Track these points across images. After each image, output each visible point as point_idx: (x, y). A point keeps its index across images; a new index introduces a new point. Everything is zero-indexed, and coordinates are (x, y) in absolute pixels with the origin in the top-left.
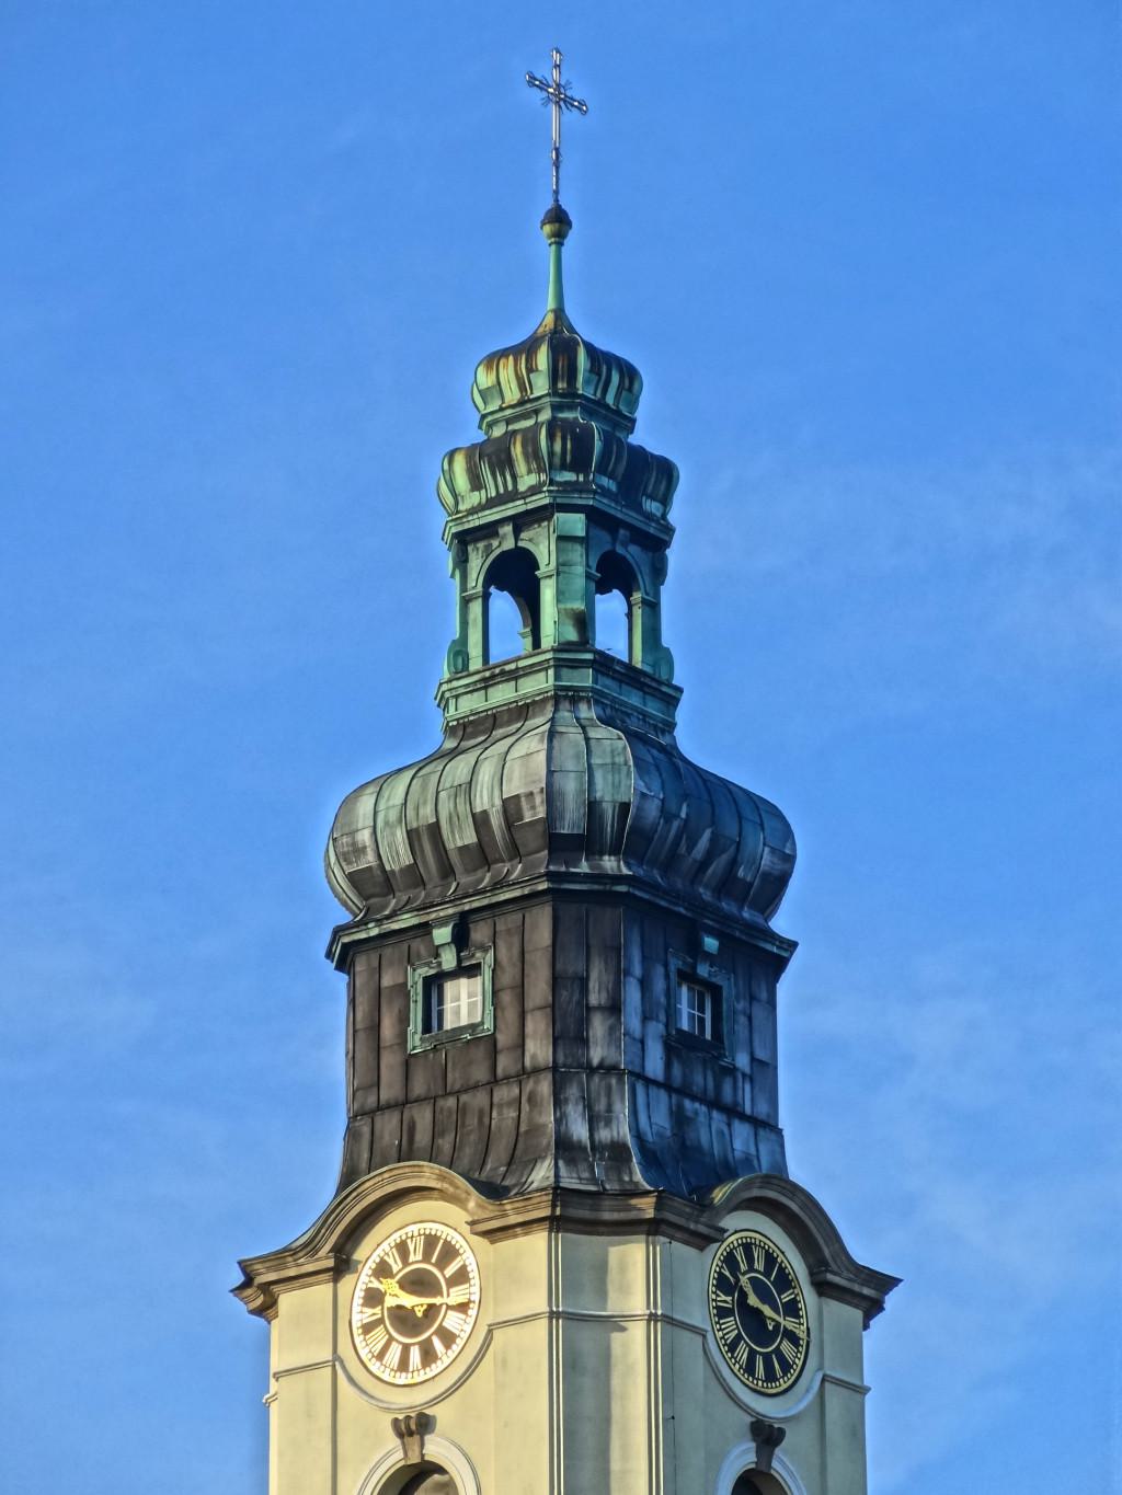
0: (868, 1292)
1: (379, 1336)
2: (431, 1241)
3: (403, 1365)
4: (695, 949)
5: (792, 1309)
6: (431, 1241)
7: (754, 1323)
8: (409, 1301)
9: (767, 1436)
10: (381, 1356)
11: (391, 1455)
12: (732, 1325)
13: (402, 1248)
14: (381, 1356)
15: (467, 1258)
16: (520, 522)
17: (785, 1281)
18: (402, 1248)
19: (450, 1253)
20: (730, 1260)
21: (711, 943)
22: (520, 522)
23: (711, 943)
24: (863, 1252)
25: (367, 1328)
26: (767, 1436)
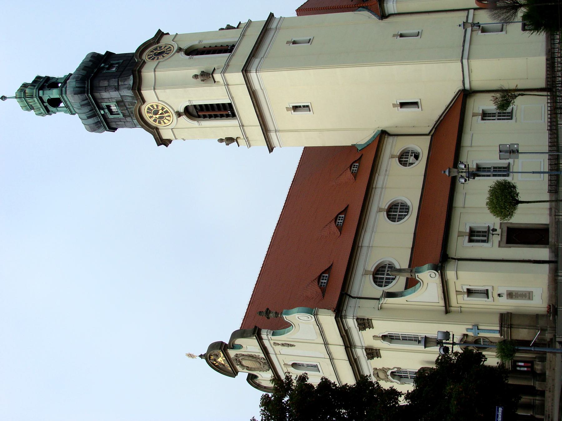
0: (160, 35)
1: (165, 121)
2: (148, 112)
3: (169, 116)
4: (103, 67)
5: (160, 47)
6: (148, 112)
7: (160, 54)
8: (157, 116)
9: (180, 50)
10: (169, 121)
11: (184, 118)
12: (160, 57)
13: (151, 117)
14: (169, 121)
15: (149, 105)
16: (43, 102)
17: (156, 49)
18: (151, 117)
19: (149, 108)
20: (149, 58)
21: (103, 65)
22: (43, 102)
23: (103, 65)
24: (151, 35)
25: (165, 123)
26: (180, 50)
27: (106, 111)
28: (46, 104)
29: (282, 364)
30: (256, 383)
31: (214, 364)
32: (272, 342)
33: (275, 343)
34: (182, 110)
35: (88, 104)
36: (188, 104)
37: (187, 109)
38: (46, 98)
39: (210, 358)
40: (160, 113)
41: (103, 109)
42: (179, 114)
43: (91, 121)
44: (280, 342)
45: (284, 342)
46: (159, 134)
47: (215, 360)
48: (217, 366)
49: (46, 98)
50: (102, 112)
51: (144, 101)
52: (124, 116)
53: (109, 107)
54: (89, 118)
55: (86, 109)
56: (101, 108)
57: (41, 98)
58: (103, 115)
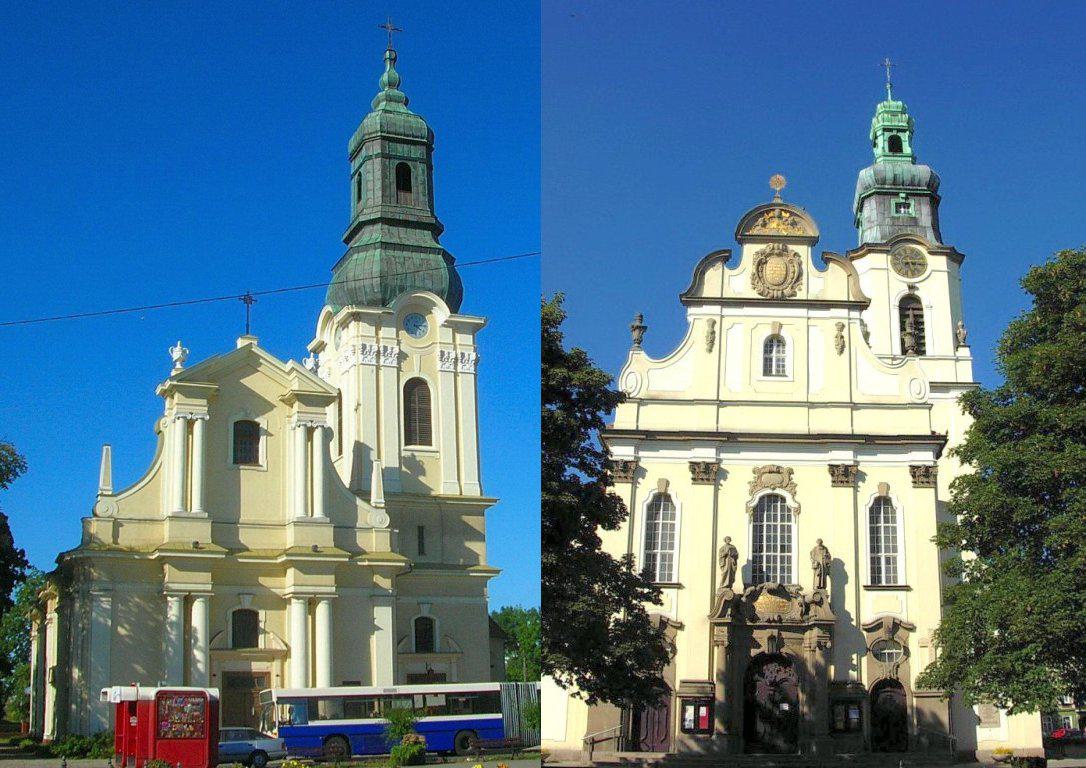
1: (899, 267)
11: (907, 291)
16: (899, 130)
22: (899, 130)
28: (895, 133)
29: (782, 321)
30: (716, 261)
31: (768, 212)
32: (846, 322)
33: (843, 326)
34: (916, 293)
35: (912, 183)
36: (924, 303)
37: (917, 300)
38: (900, 134)
39: (786, 211)
40: (911, 266)
41: (906, 198)
42: (912, 287)
43: (890, 176)
44: (845, 333)
45: (846, 339)
46: (881, 252)
47: (780, 217)
48: (762, 214)
49: (900, 134)
50: (903, 195)
51: (932, 253)
54: (895, 175)
55: (907, 177)
56: (908, 194)
57: (904, 131)
58: (897, 194)
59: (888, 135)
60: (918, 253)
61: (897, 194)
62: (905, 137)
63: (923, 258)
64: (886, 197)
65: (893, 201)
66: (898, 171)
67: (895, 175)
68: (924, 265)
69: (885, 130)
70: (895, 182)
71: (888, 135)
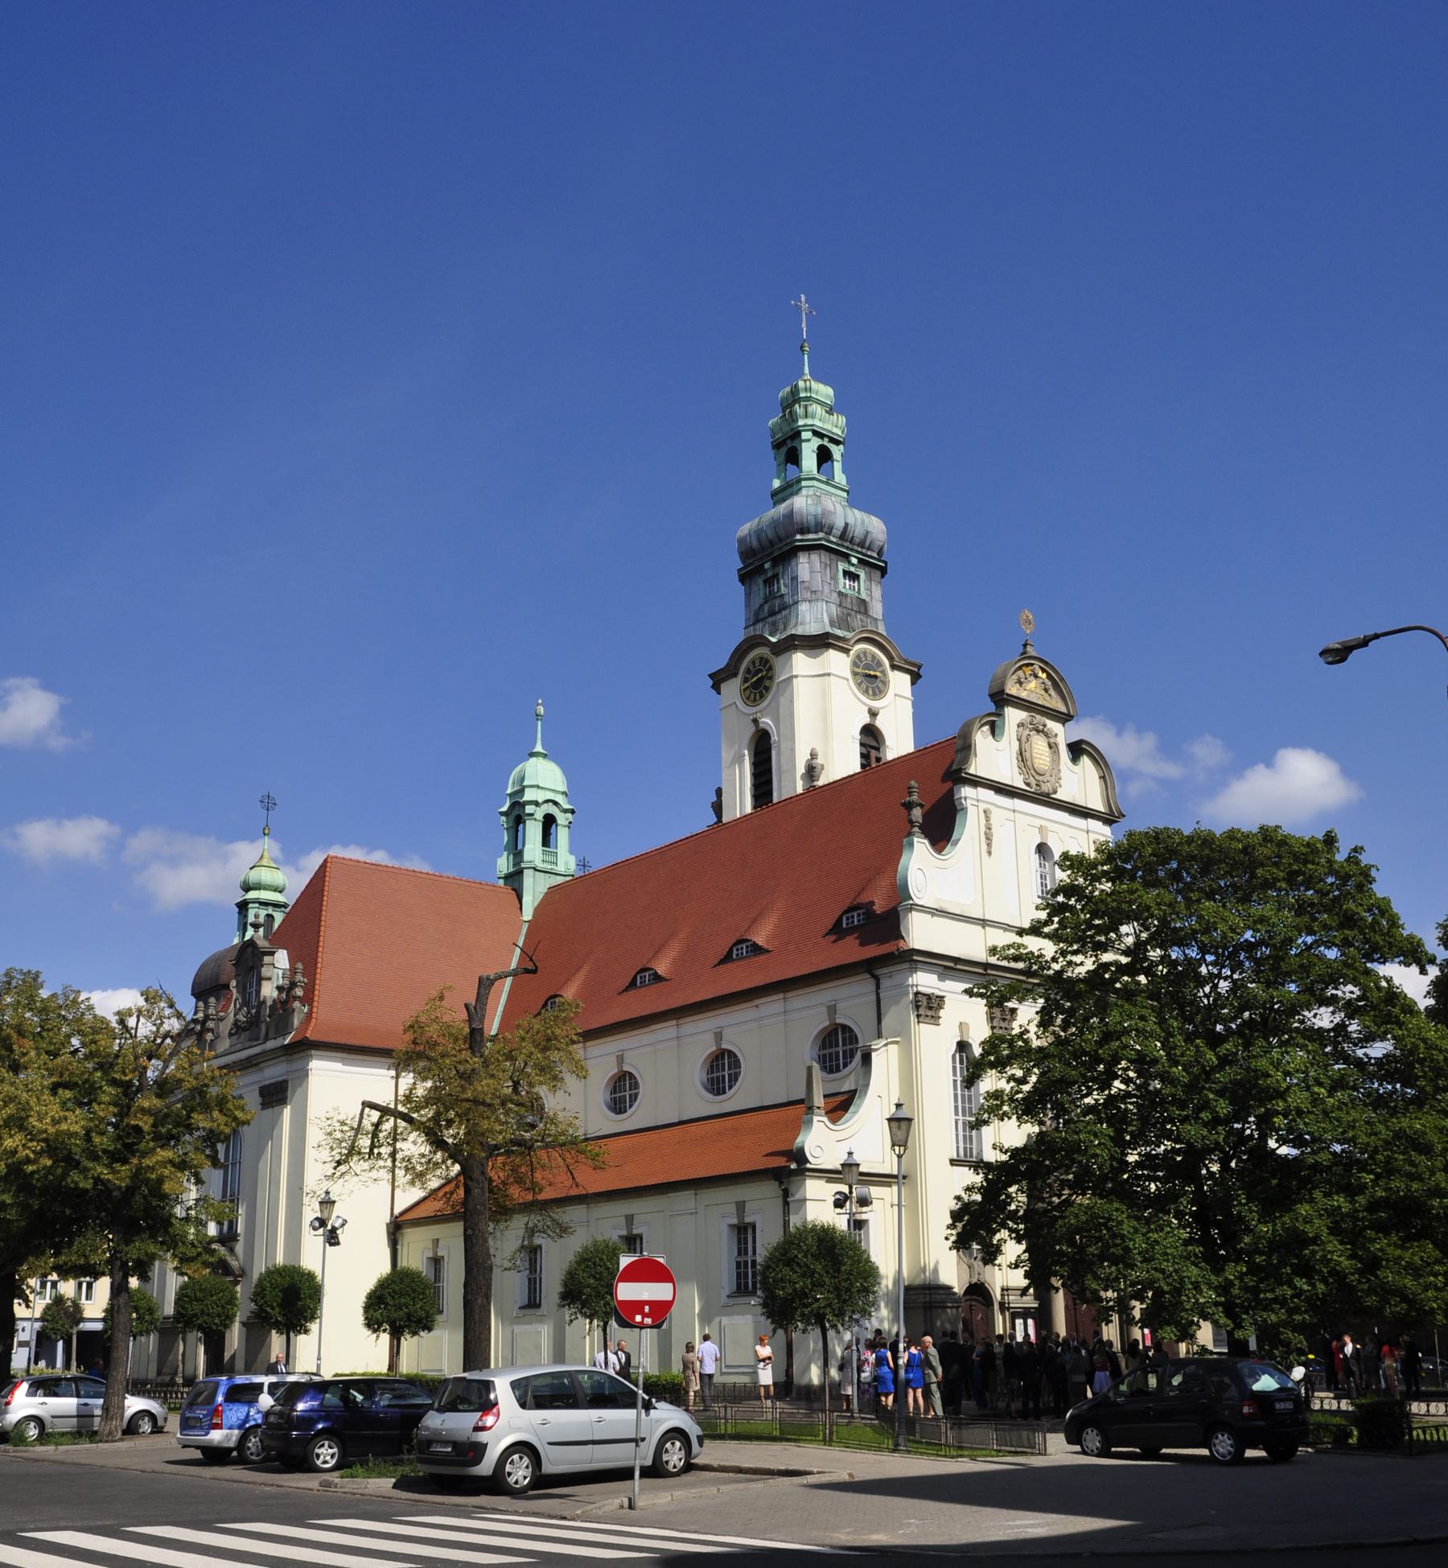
11: (867, 720)
27: (852, 569)
28: (826, 442)
38: (832, 447)
49: (832, 447)
52: (840, 594)
53: (854, 577)
54: (847, 525)
55: (858, 533)
57: (837, 442)
59: (816, 442)
60: (880, 664)
61: (846, 557)
62: (837, 451)
63: (884, 672)
64: (833, 556)
65: (842, 566)
66: (851, 521)
67: (847, 525)
68: (885, 683)
69: (816, 433)
70: (843, 536)
71: (816, 442)
